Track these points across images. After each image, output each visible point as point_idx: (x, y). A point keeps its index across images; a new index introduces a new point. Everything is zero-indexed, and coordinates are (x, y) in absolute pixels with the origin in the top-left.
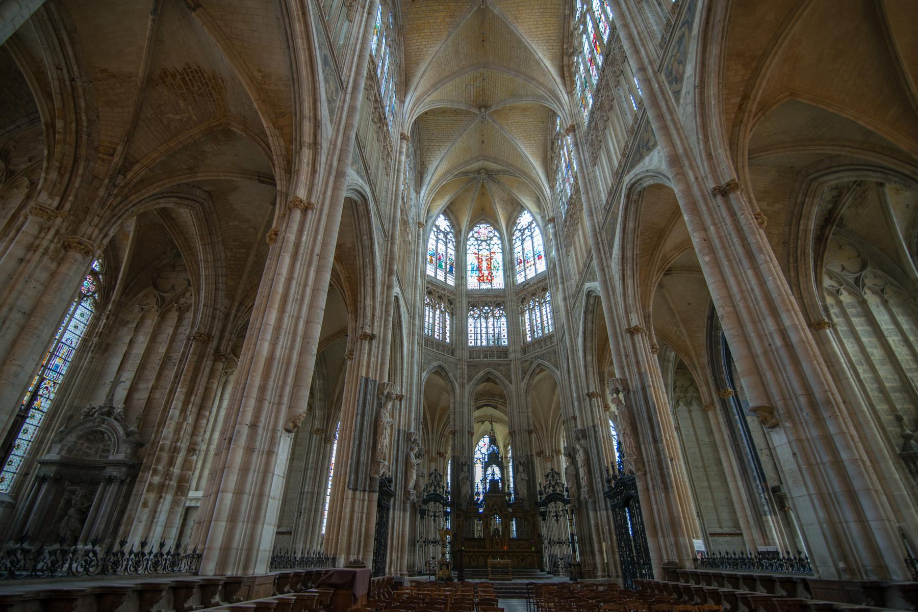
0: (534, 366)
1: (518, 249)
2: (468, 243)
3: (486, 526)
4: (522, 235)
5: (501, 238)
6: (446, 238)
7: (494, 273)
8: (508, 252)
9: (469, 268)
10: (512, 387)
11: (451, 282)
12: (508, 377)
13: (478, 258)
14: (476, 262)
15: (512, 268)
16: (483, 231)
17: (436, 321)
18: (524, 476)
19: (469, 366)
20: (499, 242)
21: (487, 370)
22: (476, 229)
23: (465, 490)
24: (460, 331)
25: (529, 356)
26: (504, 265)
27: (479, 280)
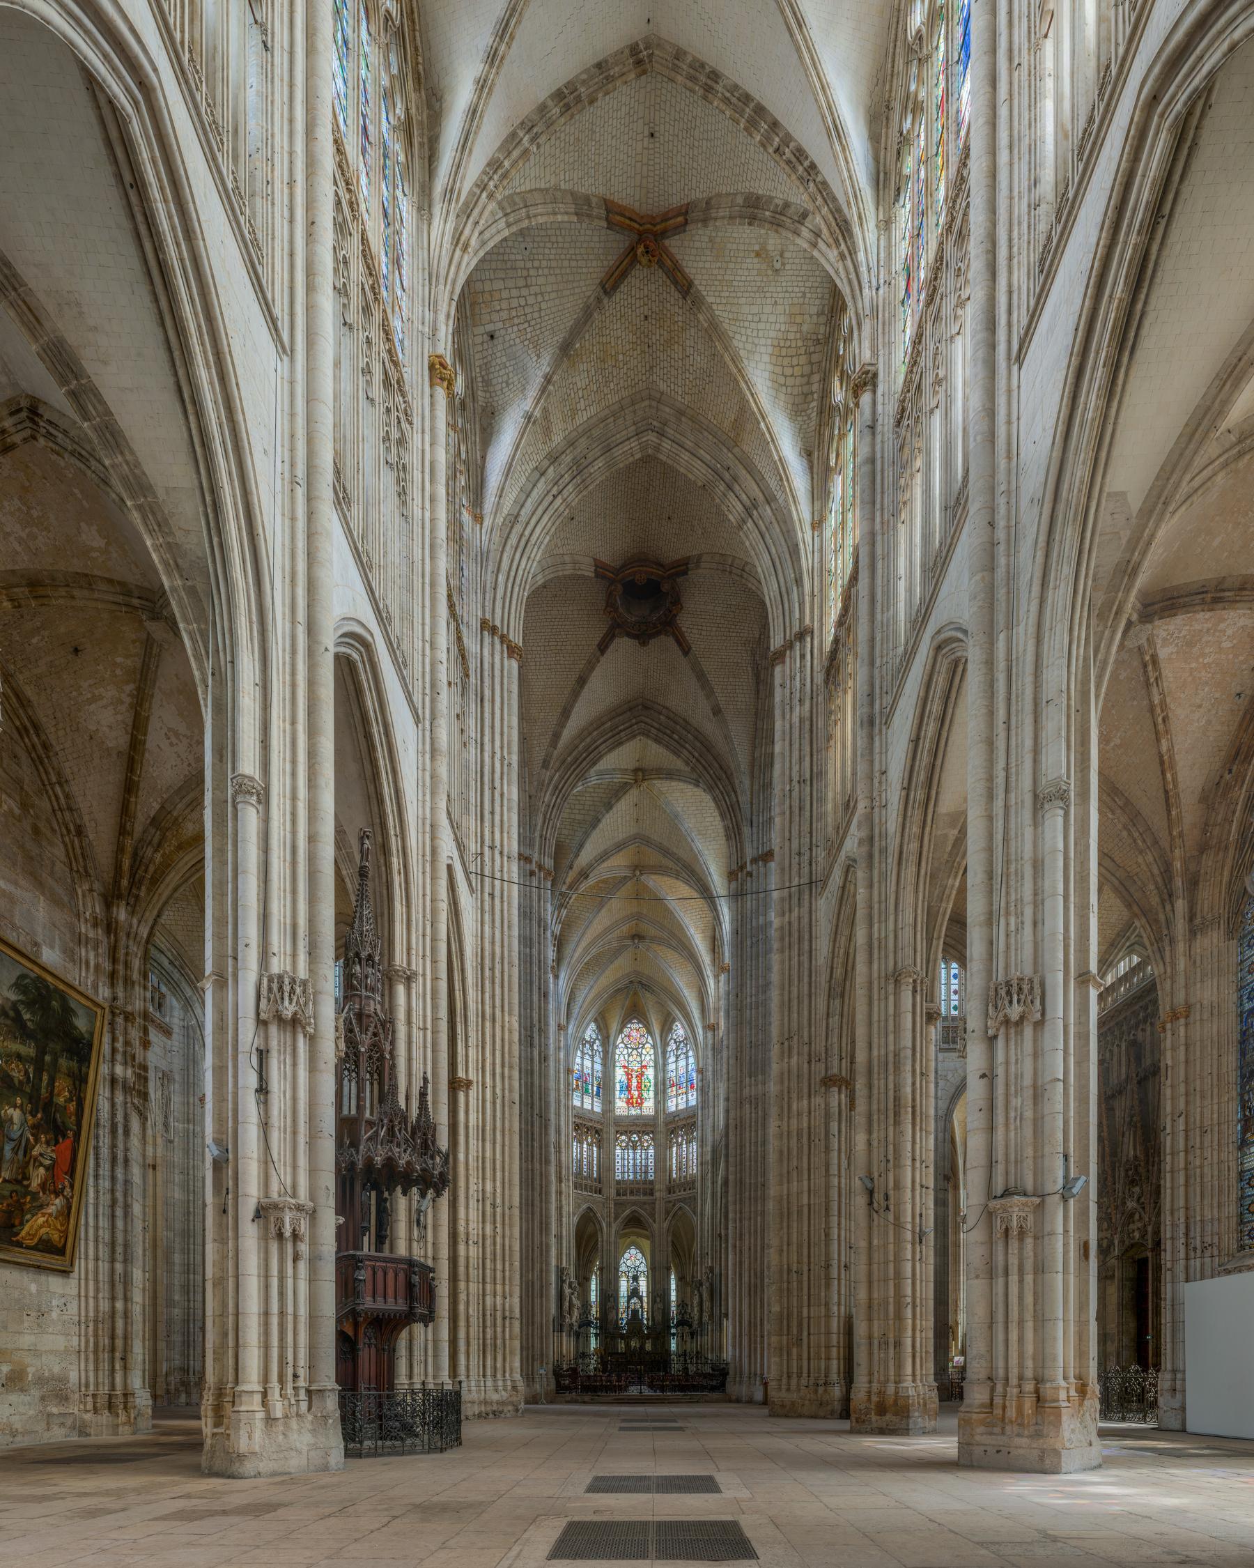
0: (676, 1208)
1: (672, 1067)
2: (617, 1051)
3: (628, 1345)
4: (677, 1049)
5: (654, 1046)
6: (592, 1049)
7: (645, 1095)
8: (661, 1067)
9: (618, 1086)
10: (656, 1226)
11: (598, 1109)
12: (652, 1215)
13: (627, 1074)
14: (624, 1079)
15: (664, 1092)
16: (634, 1033)
17: (581, 1152)
18: (660, 1306)
19: (615, 1204)
20: (652, 1051)
21: (633, 1208)
22: (626, 1031)
23: (611, 1316)
24: (606, 1164)
25: (673, 1197)
26: (656, 1085)
27: (628, 1103)
